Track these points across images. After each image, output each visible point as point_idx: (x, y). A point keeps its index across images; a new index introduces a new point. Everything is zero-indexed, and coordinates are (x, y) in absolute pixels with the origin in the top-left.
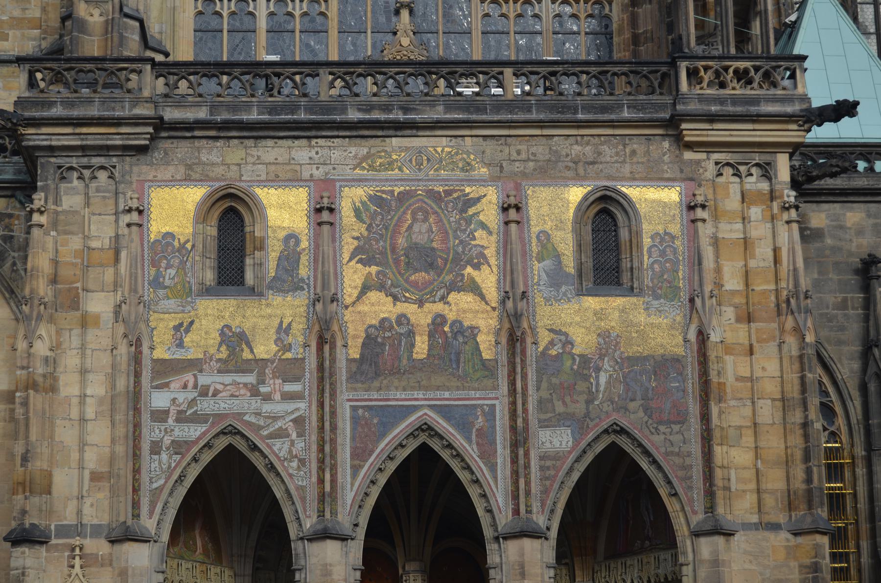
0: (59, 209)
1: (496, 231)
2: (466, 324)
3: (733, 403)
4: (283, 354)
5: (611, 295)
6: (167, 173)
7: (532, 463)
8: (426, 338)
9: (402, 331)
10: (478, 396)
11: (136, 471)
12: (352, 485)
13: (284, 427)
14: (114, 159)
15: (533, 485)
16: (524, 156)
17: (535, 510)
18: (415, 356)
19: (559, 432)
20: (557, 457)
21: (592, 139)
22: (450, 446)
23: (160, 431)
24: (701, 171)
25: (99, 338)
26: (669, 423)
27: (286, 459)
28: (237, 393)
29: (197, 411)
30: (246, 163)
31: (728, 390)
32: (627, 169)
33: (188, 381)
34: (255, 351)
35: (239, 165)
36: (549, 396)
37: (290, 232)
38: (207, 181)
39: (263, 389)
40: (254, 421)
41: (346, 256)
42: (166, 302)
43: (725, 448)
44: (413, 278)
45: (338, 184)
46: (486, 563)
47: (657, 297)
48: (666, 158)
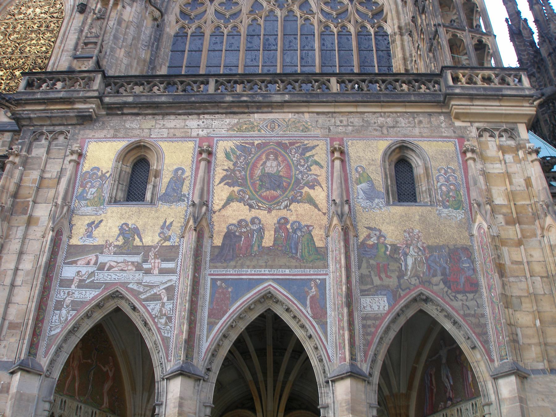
0: (30, 156)
1: (325, 166)
2: (303, 224)
3: (511, 279)
4: (163, 243)
5: (412, 206)
6: (101, 134)
7: (356, 322)
8: (273, 233)
9: (255, 228)
10: (312, 273)
11: (39, 320)
12: (208, 337)
13: (158, 293)
14: (70, 127)
15: (357, 338)
16: (345, 123)
17: (359, 359)
18: (263, 244)
19: (377, 299)
20: (376, 318)
21: (391, 114)
22: (288, 310)
23: (64, 293)
24: (468, 132)
25: (36, 232)
26: (464, 292)
27: (157, 316)
28: (126, 269)
29: (94, 280)
30: (155, 128)
31: (508, 270)
32: (417, 131)
33: (91, 260)
34: (143, 240)
35: (150, 129)
36: (368, 273)
37: (179, 167)
38: (127, 138)
39: (145, 266)
40: (135, 288)
41: (217, 180)
42: (85, 209)
43: (510, 310)
44: (265, 194)
45: (215, 139)
46: (318, 404)
47: (446, 207)
48: (443, 125)
